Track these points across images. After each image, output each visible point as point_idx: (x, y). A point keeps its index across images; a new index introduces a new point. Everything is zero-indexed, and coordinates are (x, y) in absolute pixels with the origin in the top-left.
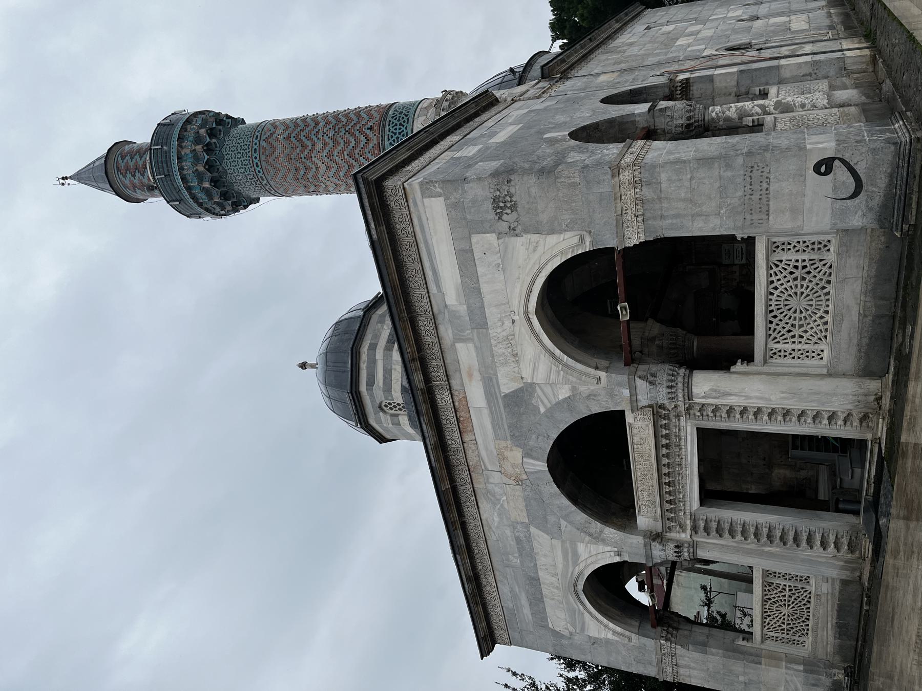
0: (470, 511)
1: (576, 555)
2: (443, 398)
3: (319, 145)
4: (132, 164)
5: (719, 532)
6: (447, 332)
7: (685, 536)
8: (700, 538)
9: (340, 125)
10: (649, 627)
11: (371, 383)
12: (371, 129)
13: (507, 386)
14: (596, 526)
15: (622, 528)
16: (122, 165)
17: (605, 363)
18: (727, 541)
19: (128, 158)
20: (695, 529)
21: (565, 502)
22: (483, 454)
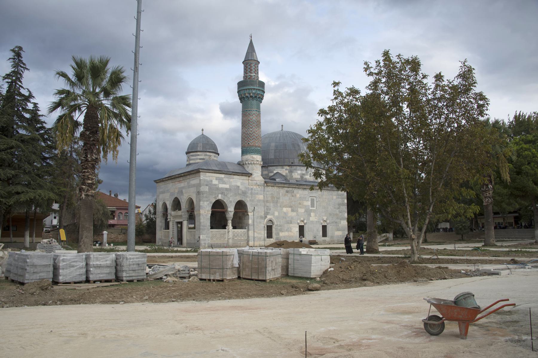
0: (170, 181)
1: (167, 201)
2: (181, 179)
3: (246, 130)
4: (248, 69)
5: (173, 225)
6: (188, 180)
7: (172, 219)
8: (172, 222)
9: (250, 135)
10: (163, 213)
11: (192, 156)
12: (249, 144)
13: (184, 191)
14: (171, 205)
15: (171, 209)
16: (247, 66)
17: (187, 207)
18: (172, 226)
19: (250, 67)
20: (173, 221)
21: (173, 200)
22: (177, 185)
